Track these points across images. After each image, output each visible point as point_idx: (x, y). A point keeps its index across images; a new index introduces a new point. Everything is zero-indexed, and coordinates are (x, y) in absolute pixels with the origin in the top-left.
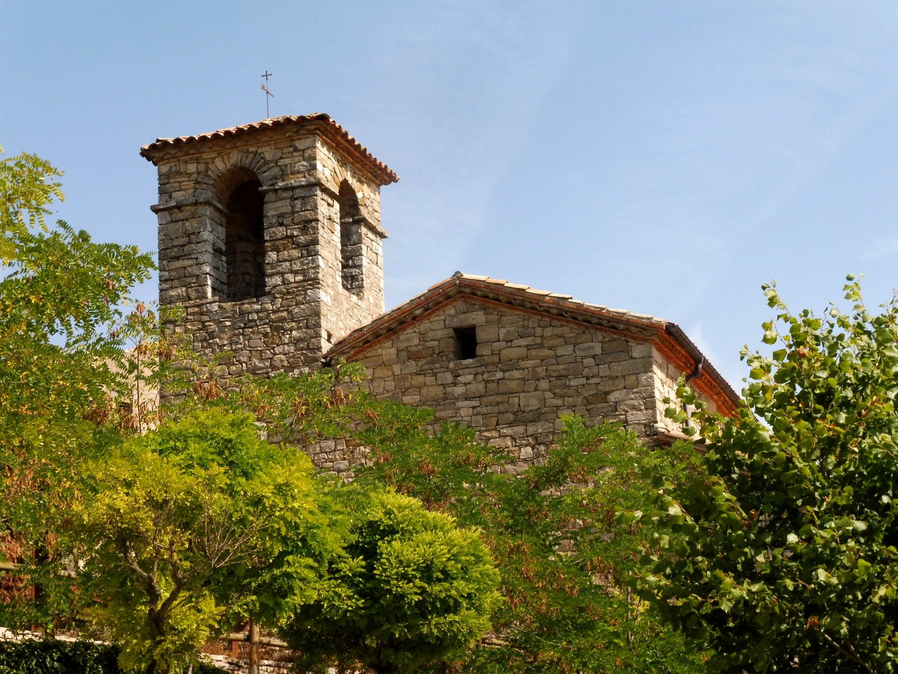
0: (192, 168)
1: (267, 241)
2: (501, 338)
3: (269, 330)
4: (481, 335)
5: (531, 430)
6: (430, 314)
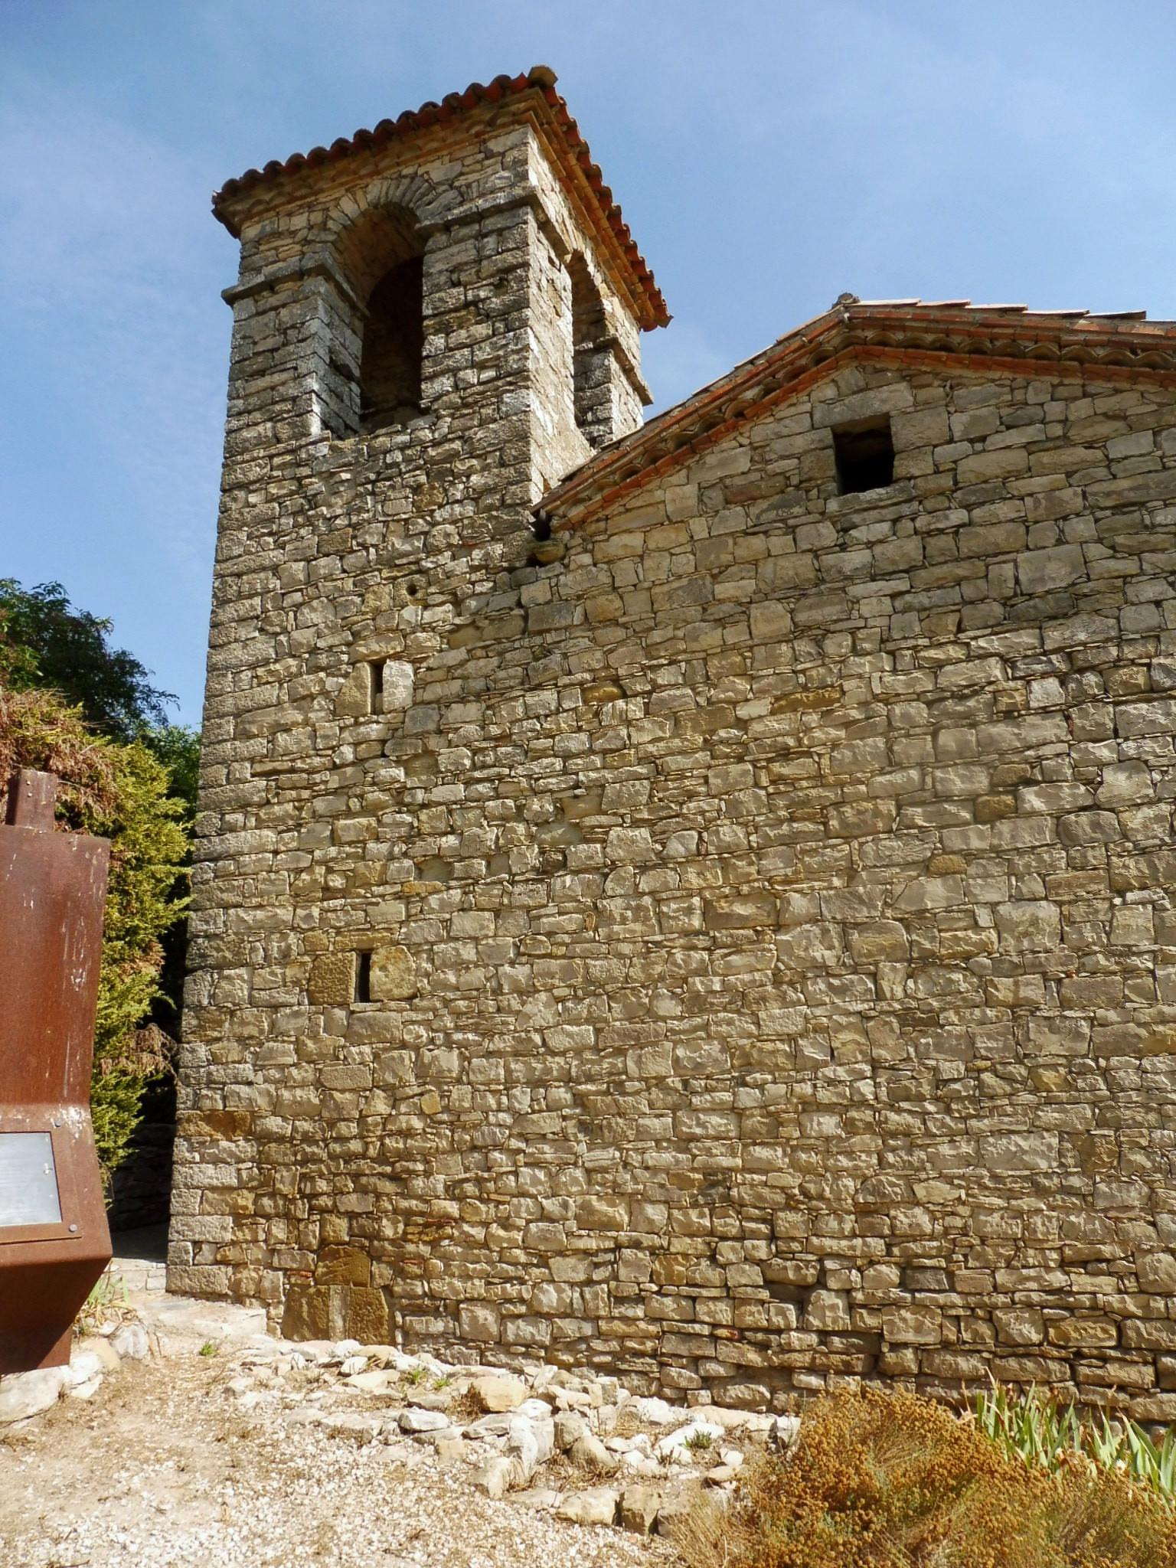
0: (299, 222)
1: (427, 317)
2: (957, 435)
3: (423, 479)
4: (903, 434)
5: (1055, 636)
6: (776, 403)
